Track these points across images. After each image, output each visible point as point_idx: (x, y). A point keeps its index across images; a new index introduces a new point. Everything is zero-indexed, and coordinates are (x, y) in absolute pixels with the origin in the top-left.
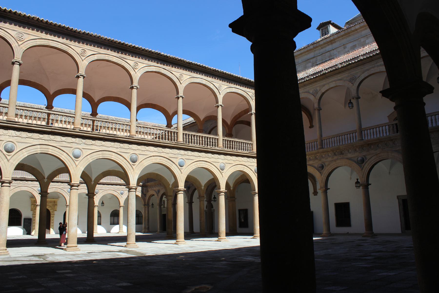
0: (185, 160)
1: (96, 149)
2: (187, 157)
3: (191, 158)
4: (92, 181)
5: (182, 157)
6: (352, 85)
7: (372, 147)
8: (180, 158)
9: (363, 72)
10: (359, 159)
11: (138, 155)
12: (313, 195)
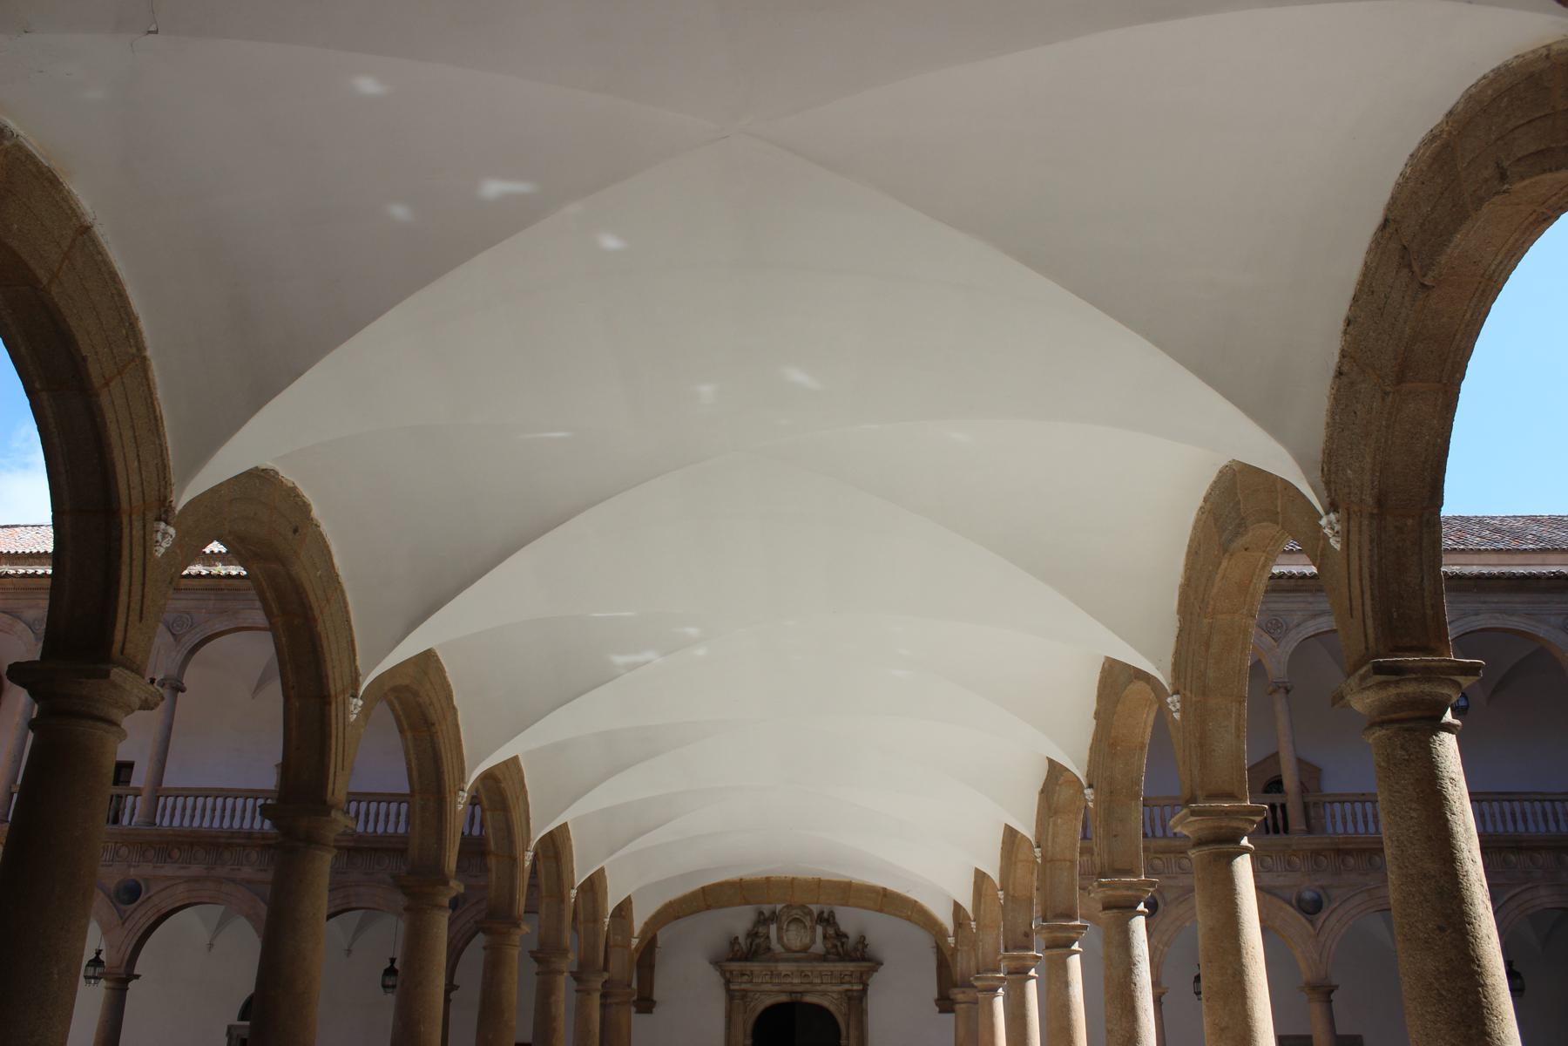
4: (463, 790)
6: (1275, 644)
7: (1351, 861)
9: (1315, 616)
10: (1308, 895)
12: (937, 1009)
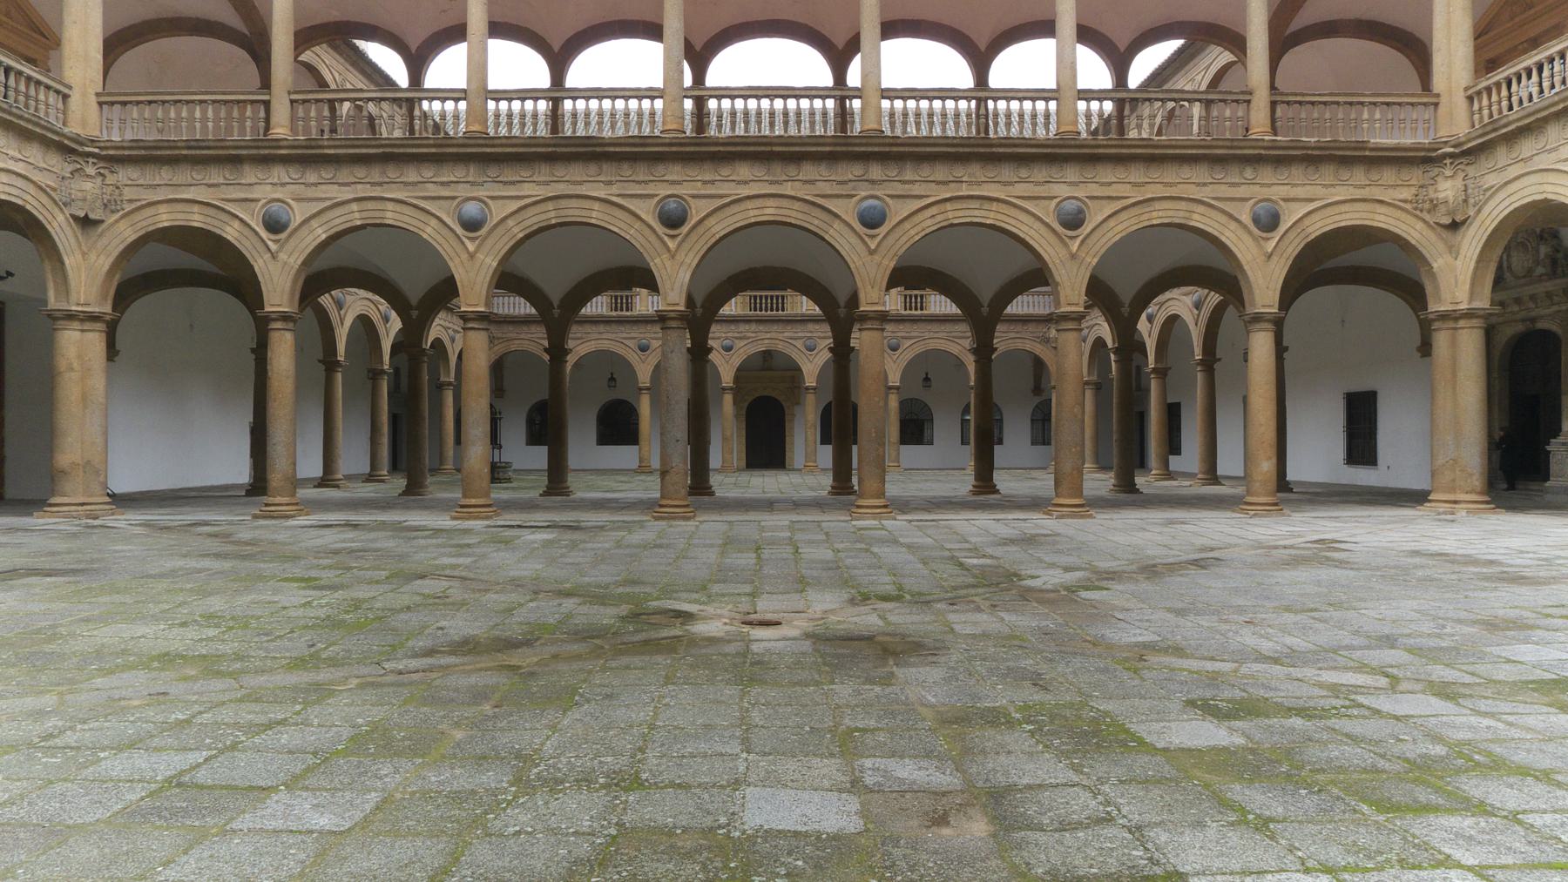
0: (888, 199)
1: (535, 193)
2: (899, 189)
3: (917, 190)
5: (873, 189)
8: (864, 194)
11: (689, 199)
